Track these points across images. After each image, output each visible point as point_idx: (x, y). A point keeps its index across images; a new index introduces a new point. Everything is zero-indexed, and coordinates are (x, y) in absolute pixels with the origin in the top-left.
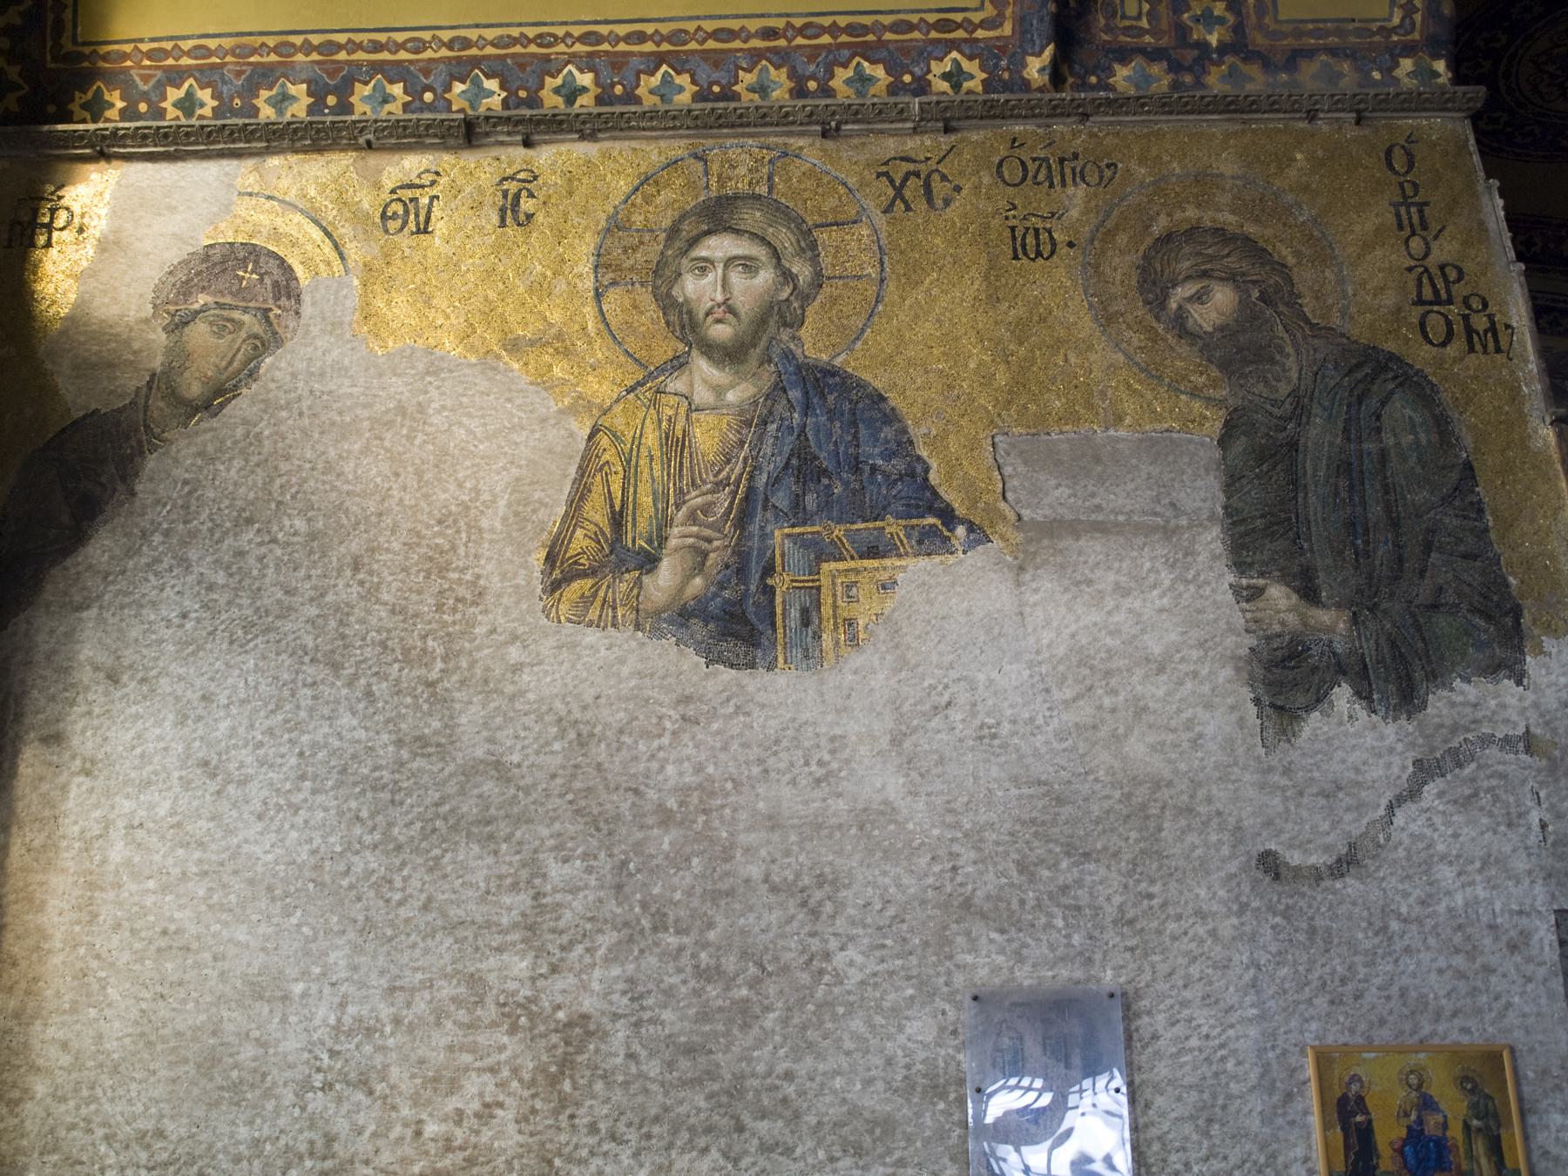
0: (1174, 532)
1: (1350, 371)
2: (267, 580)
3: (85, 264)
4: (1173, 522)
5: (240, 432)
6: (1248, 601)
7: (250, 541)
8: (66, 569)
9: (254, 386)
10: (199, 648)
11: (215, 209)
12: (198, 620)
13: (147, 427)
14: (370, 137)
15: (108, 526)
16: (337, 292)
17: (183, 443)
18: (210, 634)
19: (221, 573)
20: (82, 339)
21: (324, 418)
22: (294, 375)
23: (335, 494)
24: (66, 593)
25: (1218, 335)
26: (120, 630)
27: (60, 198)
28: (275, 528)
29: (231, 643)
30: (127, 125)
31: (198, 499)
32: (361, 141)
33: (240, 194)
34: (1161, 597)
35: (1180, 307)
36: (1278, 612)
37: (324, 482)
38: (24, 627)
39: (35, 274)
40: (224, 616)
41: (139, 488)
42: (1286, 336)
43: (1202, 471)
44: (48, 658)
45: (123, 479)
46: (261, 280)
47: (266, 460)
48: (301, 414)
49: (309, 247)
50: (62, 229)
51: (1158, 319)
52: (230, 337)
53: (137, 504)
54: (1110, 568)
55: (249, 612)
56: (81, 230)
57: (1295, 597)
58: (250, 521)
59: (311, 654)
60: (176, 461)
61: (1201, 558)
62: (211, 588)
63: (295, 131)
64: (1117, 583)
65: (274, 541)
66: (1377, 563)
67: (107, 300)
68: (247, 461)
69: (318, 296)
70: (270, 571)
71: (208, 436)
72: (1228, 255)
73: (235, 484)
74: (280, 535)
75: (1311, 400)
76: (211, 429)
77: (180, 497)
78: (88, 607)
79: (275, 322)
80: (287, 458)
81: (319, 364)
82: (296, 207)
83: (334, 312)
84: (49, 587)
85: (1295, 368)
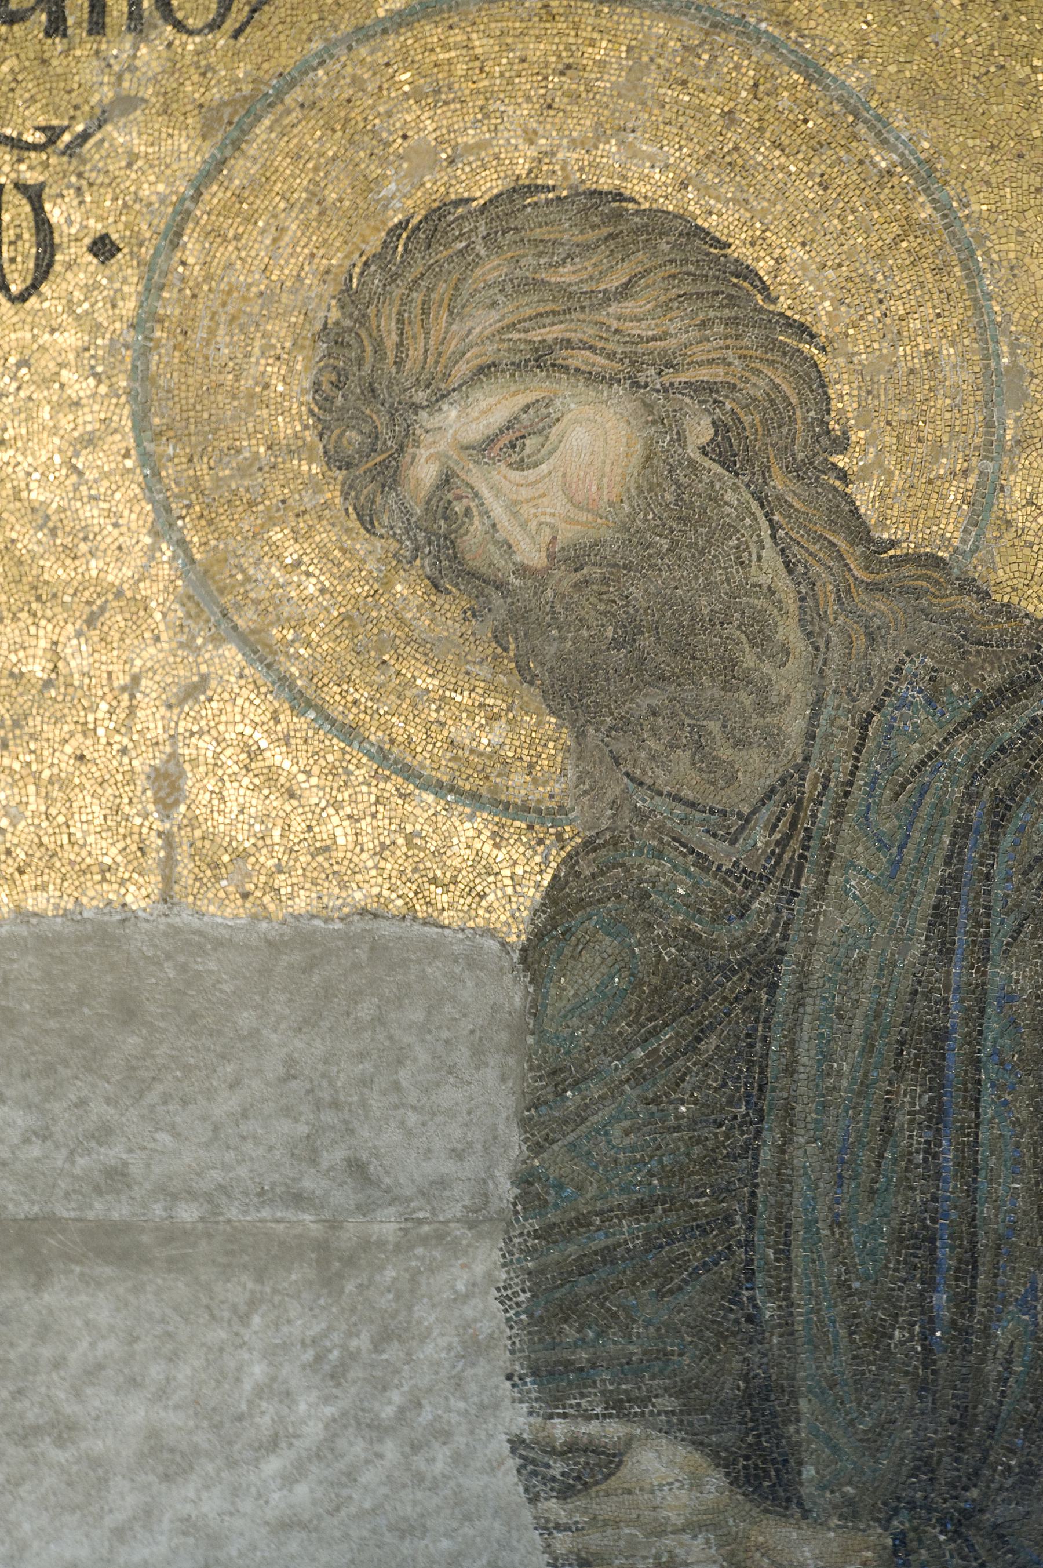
0: (350, 1261)
1: (981, 712)
4: (353, 1227)
6: (565, 1493)
25: (564, 579)
34: (288, 1480)
35: (447, 480)
36: (659, 1530)
42: (784, 584)
43: (462, 1056)
51: (367, 520)
54: (134, 1383)
57: (715, 1481)
61: (429, 1349)
64: (154, 1434)
66: (992, 1370)
72: (625, 291)
75: (839, 814)
85: (800, 696)
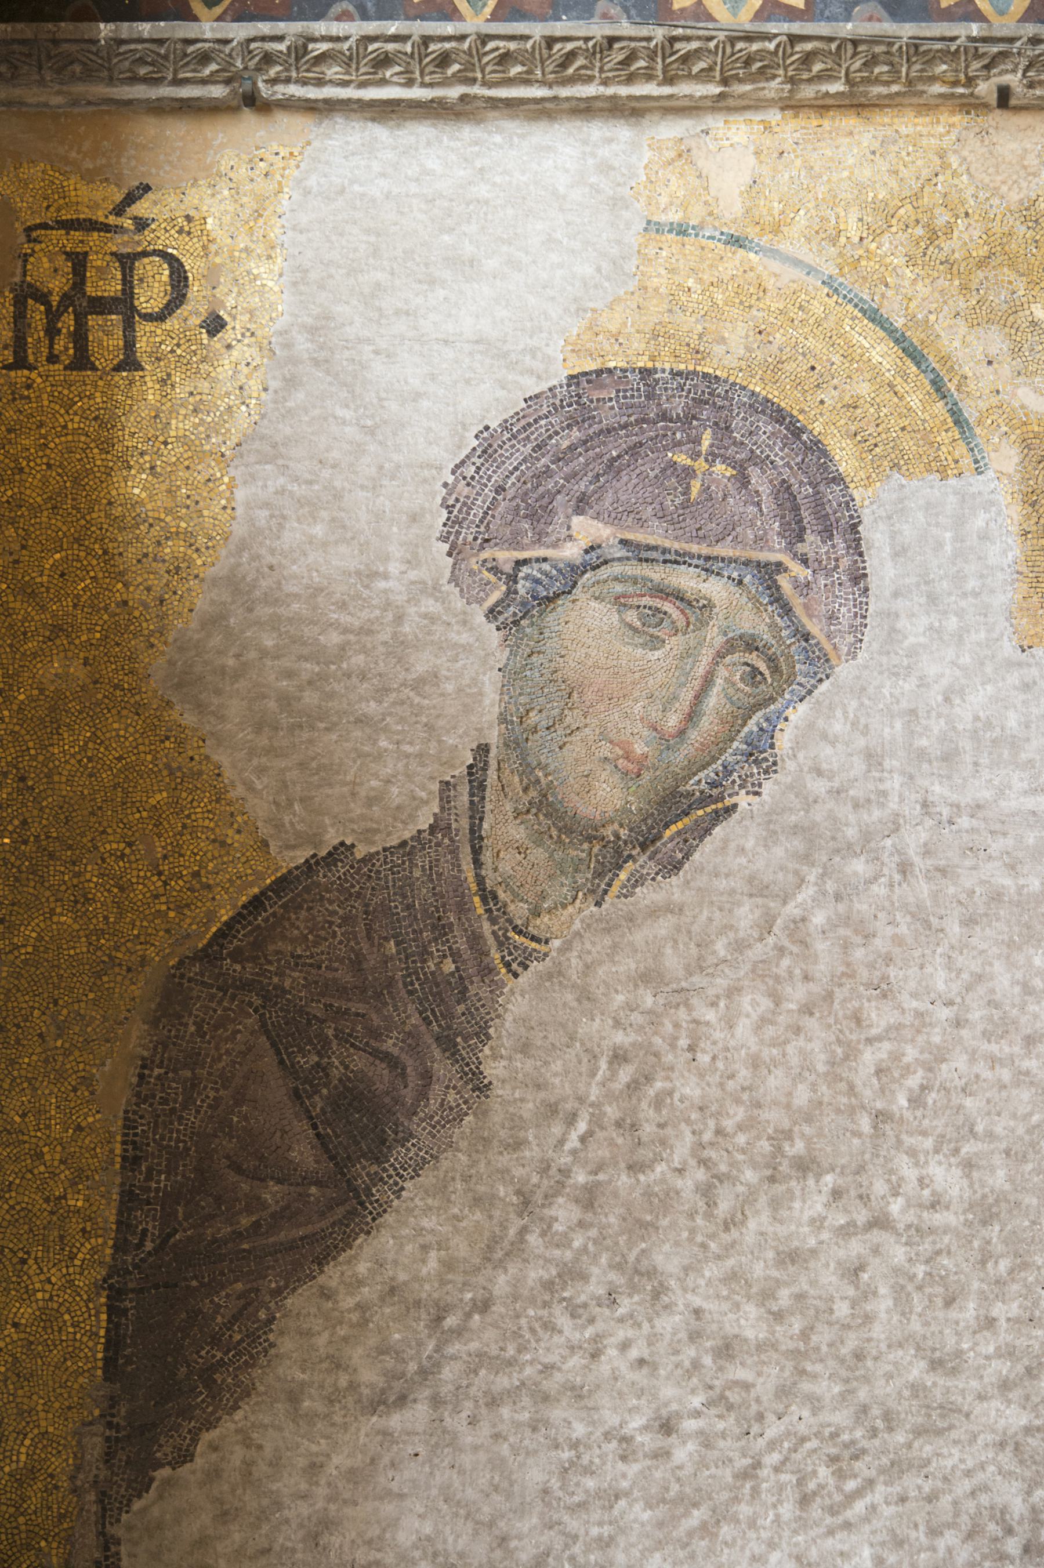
2: (878, 1331)
3: (242, 420)
5: (746, 915)
7: (817, 1223)
8: (326, 1294)
9: (767, 787)
10: (720, 1516)
11: (588, 270)
12: (706, 1440)
13: (488, 896)
14: (1013, 80)
15: (427, 1178)
16: (959, 522)
17: (597, 945)
18: (745, 1475)
19: (751, 1310)
20: (269, 643)
21: (968, 881)
22: (873, 758)
23: (1026, 1095)
24: (337, 1365)
26: (498, 1464)
27: (141, 224)
28: (880, 1187)
29: (805, 1501)
30: (337, 28)
31: (658, 1103)
32: (985, 89)
33: (653, 227)
37: (993, 1061)
38: (238, 1455)
39: (106, 446)
40: (774, 1429)
41: (493, 1070)
44: (313, 1539)
45: (448, 1044)
46: (743, 480)
47: (829, 996)
48: (905, 868)
49: (864, 389)
50: (160, 317)
52: (675, 644)
53: (497, 1117)
55: (841, 1417)
56: (215, 325)
58: (804, 1166)
59: (1023, 1532)
60: (585, 995)
62: (726, 1350)
63: (808, 59)
65: (881, 1222)
67: (318, 530)
68: (777, 1000)
69: (908, 532)
70: (883, 1305)
71: (664, 926)
73: (755, 1063)
74: (895, 1207)
76: (670, 909)
77: (611, 1097)
78: (402, 1400)
79: (797, 603)
80: (883, 990)
81: (938, 726)
82: (810, 270)
83: (959, 578)
84: (286, 1345)
